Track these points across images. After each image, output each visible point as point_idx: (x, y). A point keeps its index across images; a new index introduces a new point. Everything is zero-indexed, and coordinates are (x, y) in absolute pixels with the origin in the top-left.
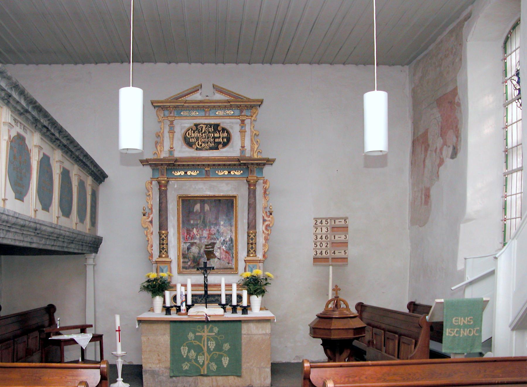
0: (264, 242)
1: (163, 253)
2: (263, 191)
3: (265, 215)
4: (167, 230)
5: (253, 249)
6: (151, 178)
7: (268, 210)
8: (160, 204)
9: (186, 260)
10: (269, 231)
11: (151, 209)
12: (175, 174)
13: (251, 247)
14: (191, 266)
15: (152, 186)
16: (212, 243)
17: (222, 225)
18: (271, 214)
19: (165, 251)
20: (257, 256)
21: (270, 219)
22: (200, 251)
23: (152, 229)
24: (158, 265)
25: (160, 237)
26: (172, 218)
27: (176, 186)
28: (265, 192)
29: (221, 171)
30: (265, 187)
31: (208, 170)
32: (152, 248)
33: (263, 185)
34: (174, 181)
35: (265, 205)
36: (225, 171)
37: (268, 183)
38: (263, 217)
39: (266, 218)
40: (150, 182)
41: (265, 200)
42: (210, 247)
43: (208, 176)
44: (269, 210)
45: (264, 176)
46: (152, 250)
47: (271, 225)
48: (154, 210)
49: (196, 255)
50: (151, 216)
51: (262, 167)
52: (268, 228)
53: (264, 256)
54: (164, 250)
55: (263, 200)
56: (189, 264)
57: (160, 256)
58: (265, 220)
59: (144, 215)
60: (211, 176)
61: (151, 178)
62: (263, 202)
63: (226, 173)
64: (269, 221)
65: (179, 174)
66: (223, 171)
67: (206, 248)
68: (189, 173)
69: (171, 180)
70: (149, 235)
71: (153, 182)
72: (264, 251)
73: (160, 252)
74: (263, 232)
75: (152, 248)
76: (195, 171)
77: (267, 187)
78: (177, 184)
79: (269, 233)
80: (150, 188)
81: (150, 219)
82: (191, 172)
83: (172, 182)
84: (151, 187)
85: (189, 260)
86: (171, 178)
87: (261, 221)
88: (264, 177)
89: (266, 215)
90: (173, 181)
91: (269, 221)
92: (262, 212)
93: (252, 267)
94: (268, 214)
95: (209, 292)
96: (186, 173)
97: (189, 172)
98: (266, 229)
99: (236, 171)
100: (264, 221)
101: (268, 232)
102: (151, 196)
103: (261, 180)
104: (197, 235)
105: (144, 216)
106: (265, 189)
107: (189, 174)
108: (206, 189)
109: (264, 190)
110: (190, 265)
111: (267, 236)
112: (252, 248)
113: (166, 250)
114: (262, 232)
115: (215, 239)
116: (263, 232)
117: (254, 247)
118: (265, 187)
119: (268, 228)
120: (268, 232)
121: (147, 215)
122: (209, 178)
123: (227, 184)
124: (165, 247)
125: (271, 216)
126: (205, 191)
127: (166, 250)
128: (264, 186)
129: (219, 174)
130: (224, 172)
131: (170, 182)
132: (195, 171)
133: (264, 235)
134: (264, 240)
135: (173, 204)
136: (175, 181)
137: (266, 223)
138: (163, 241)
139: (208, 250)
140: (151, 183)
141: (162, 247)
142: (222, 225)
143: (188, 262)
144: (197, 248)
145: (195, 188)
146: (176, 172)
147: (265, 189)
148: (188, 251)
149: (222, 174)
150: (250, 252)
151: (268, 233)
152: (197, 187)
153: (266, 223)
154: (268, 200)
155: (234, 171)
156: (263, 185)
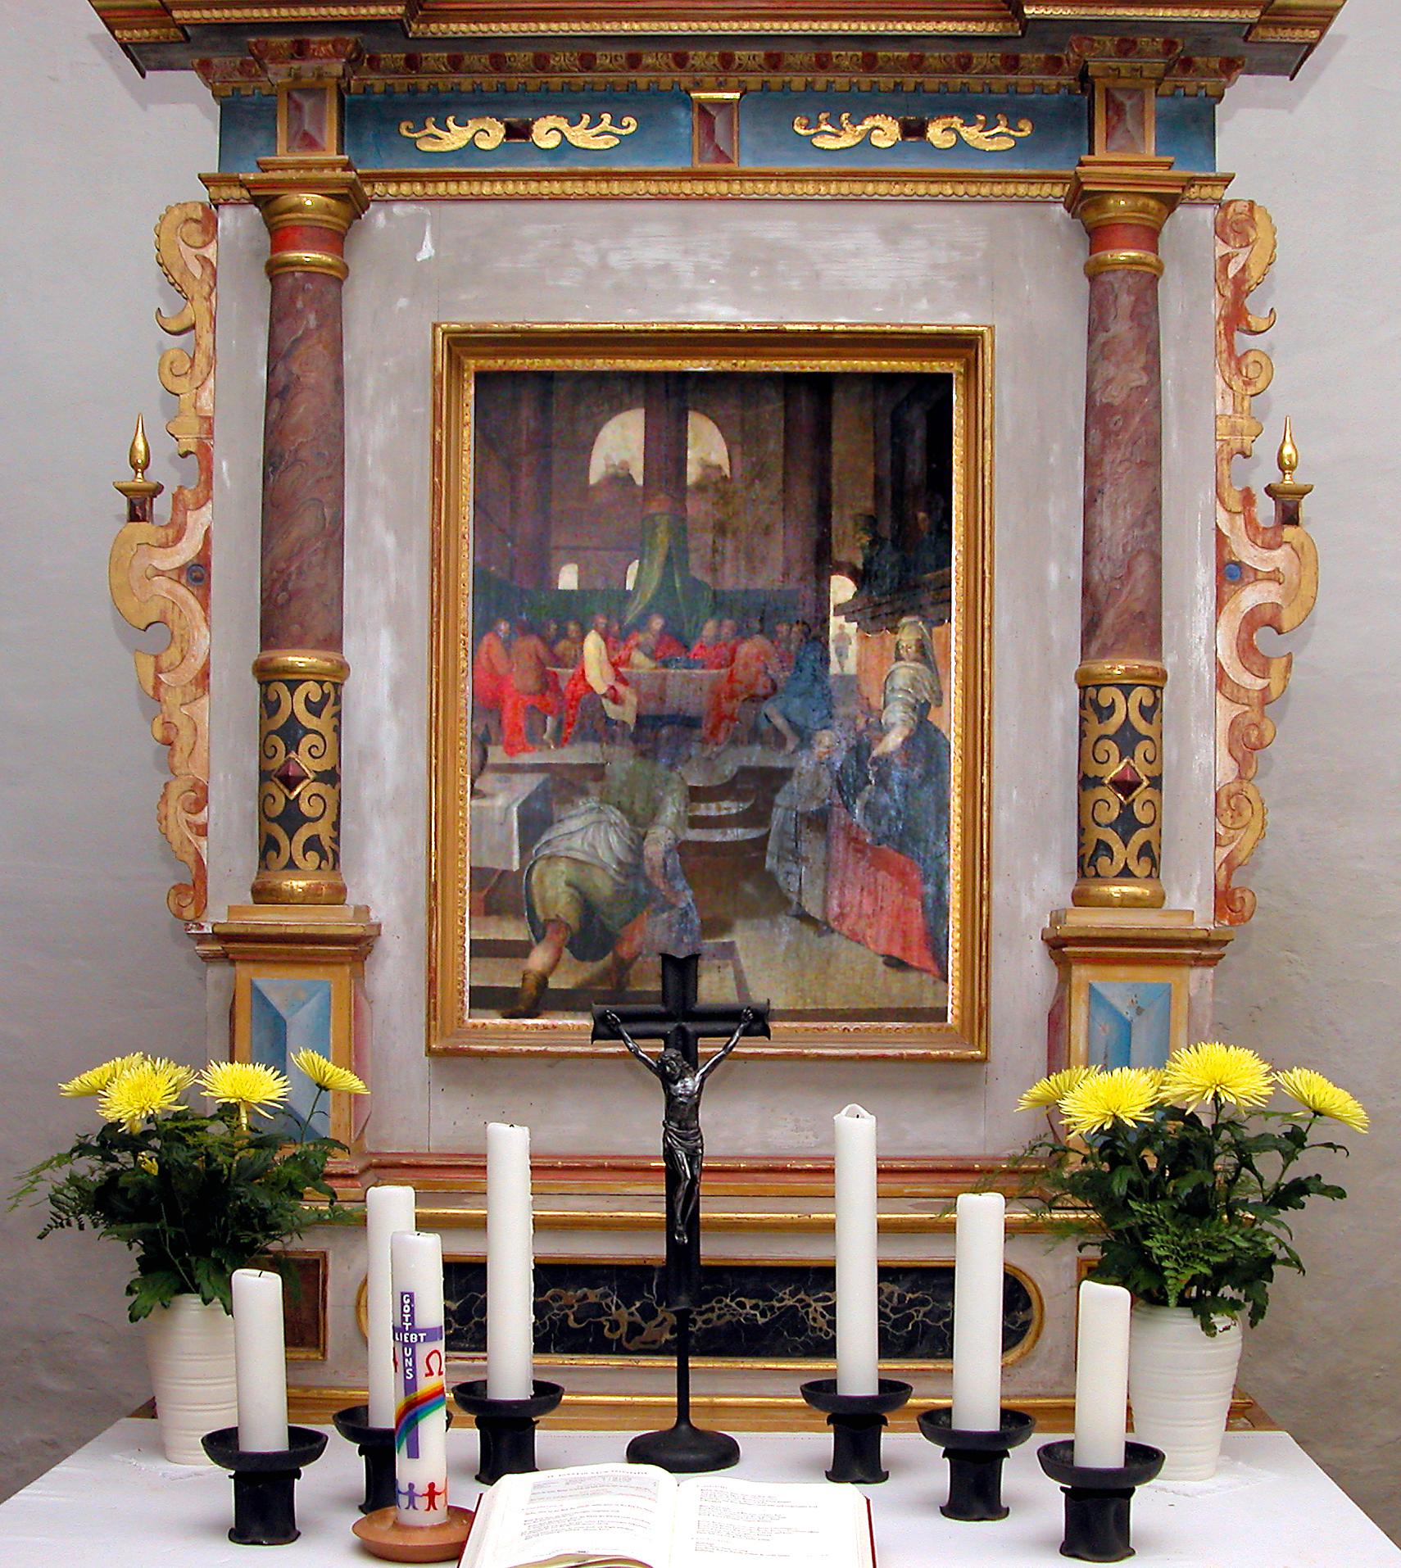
0: (1226, 769)
1: (291, 865)
2: (1215, 308)
3: (1240, 521)
4: (333, 641)
5: (1139, 838)
6: (207, 181)
7: (1264, 474)
8: (276, 404)
9: (513, 931)
10: (1277, 668)
11: (204, 455)
12: (426, 146)
13: (1115, 812)
14: (553, 983)
15: (210, 252)
16: (745, 772)
17: (840, 609)
18: (1289, 516)
19: (313, 844)
20: (1166, 906)
21: (1279, 558)
22: (637, 848)
23: (202, 641)
24: (244, 972)
25: (270, 706)
26: (390, 541)
27: (427, 251)
28: (1235, 319)
29: (835, 121)
30: (1232, 271)
31: (724, 105)
32: (200, 818)
33: (1222, 249)
34: (412, 208)
35: (1234, 430)
36: (878, 121)
37: (1260, 234)
38: (1221, 539)
39: (1247, 553)
40: (199, 214)
41: (1237, 384)
42: (730, 807)
43: (722, 156)
44: (1273, 476)
45: (1221, 168)
46: (202, 830)
47: (1287, 619)
48: (223, 467)
49: (603, 885)
50: (199, 520)
51: (1210, 83)
52: (1263, 638)
53: (1224, 900)
54: (304, 834)
55: (1220, 384)
56: (539, 959)
57: (263, 894)
58: (1239, 565)
59: (139, 507)
60: (747, 165)
61: (207, 181)
62: (1223, 405)
63: (886, 131)
64: (1274, 577)
65: (455, 137)
66: (856, 121)
67: (696, 822)
68: (546, 133)
69: (384, 201)
70: (172, 698)
71: (227, 218)
72: (1223, 853)
73: (269, 846)
74: (1221, 677)
75: (200, 818)
76: (607, 117)
77: (1254, 273)
78: (436, 244)
79: (1275, 691)
80: (196, 269)
81: (187, 550)
82: (563, 124)
83: (389, 217)
84: (205, 261)
85: (539, 931)
86: (387, 178)
87: (1204, 576)
88: (1227, 180)
89: (1250, 521)
90: (397, 209)
91: (1274, 577)
92: (1211, 493)
93: (1128, 1013)
94: (1266, 510)
95: (712, 1250)
96: (518, 132)
97: (551, 121)
98: (1246, 650)
99: (968, 123)
100: (1230, 573)
101: (1260, 683)
102: (207, 340)
103: (1203, 202)
104: (616, 699)
105: (134, 517)
106: (1239, 282)
107: (551, 142)
108: (702, 273)
109: (1228, 293)
110: (543, 980)
111: (1254, 716)
112: (1127, 824)
113: (323, 829)
114: (1209, 677)
115: (780, 741)
116: (1221, 677)
117: (1142, 814)
118: (1232, 271)
119: (1263, 638)
120: (1260, 683)
121: (162, 506)
122: (730, 177)
123: (891, 236)
124: (304, 807)
125: (1289, 532)
126: (692, 297)
127: (323, 829)
128: (1226, 260)
129: (819, 142)
130: (868, 123)
131: (378, 218)
132: (607, 117)
133: (1226, 712)
134: (1223, 751)
135: (394, 410)
136: (425, 209)
137: (1250, 597)
138: (293, 745)
139: (717, 836)
140: (208, 223)
141: (279, 807)
142: (840, 609)
143: (520, 950)
144: (616, 816)
145: (604, 266)
146: (432, 129)
147: (1239, 282)
148: (524, 849)
149: (847, 141)
150: (1103, 861)
151: (1265, 690)
152: (614, 259)
153: (1250, 597)
154: (1260, 385)
155: (957, 122)
156: (1222, 249)
